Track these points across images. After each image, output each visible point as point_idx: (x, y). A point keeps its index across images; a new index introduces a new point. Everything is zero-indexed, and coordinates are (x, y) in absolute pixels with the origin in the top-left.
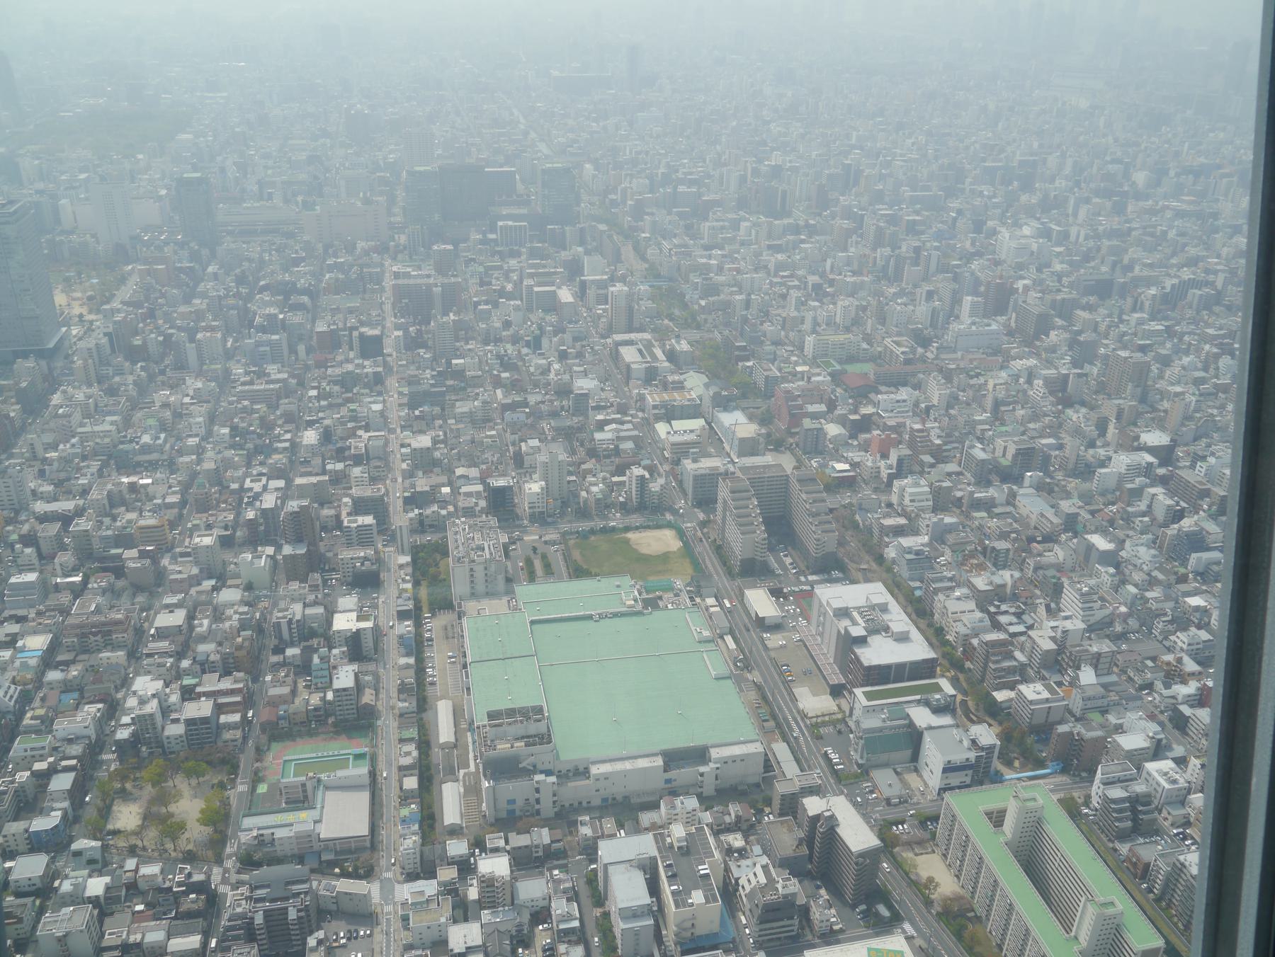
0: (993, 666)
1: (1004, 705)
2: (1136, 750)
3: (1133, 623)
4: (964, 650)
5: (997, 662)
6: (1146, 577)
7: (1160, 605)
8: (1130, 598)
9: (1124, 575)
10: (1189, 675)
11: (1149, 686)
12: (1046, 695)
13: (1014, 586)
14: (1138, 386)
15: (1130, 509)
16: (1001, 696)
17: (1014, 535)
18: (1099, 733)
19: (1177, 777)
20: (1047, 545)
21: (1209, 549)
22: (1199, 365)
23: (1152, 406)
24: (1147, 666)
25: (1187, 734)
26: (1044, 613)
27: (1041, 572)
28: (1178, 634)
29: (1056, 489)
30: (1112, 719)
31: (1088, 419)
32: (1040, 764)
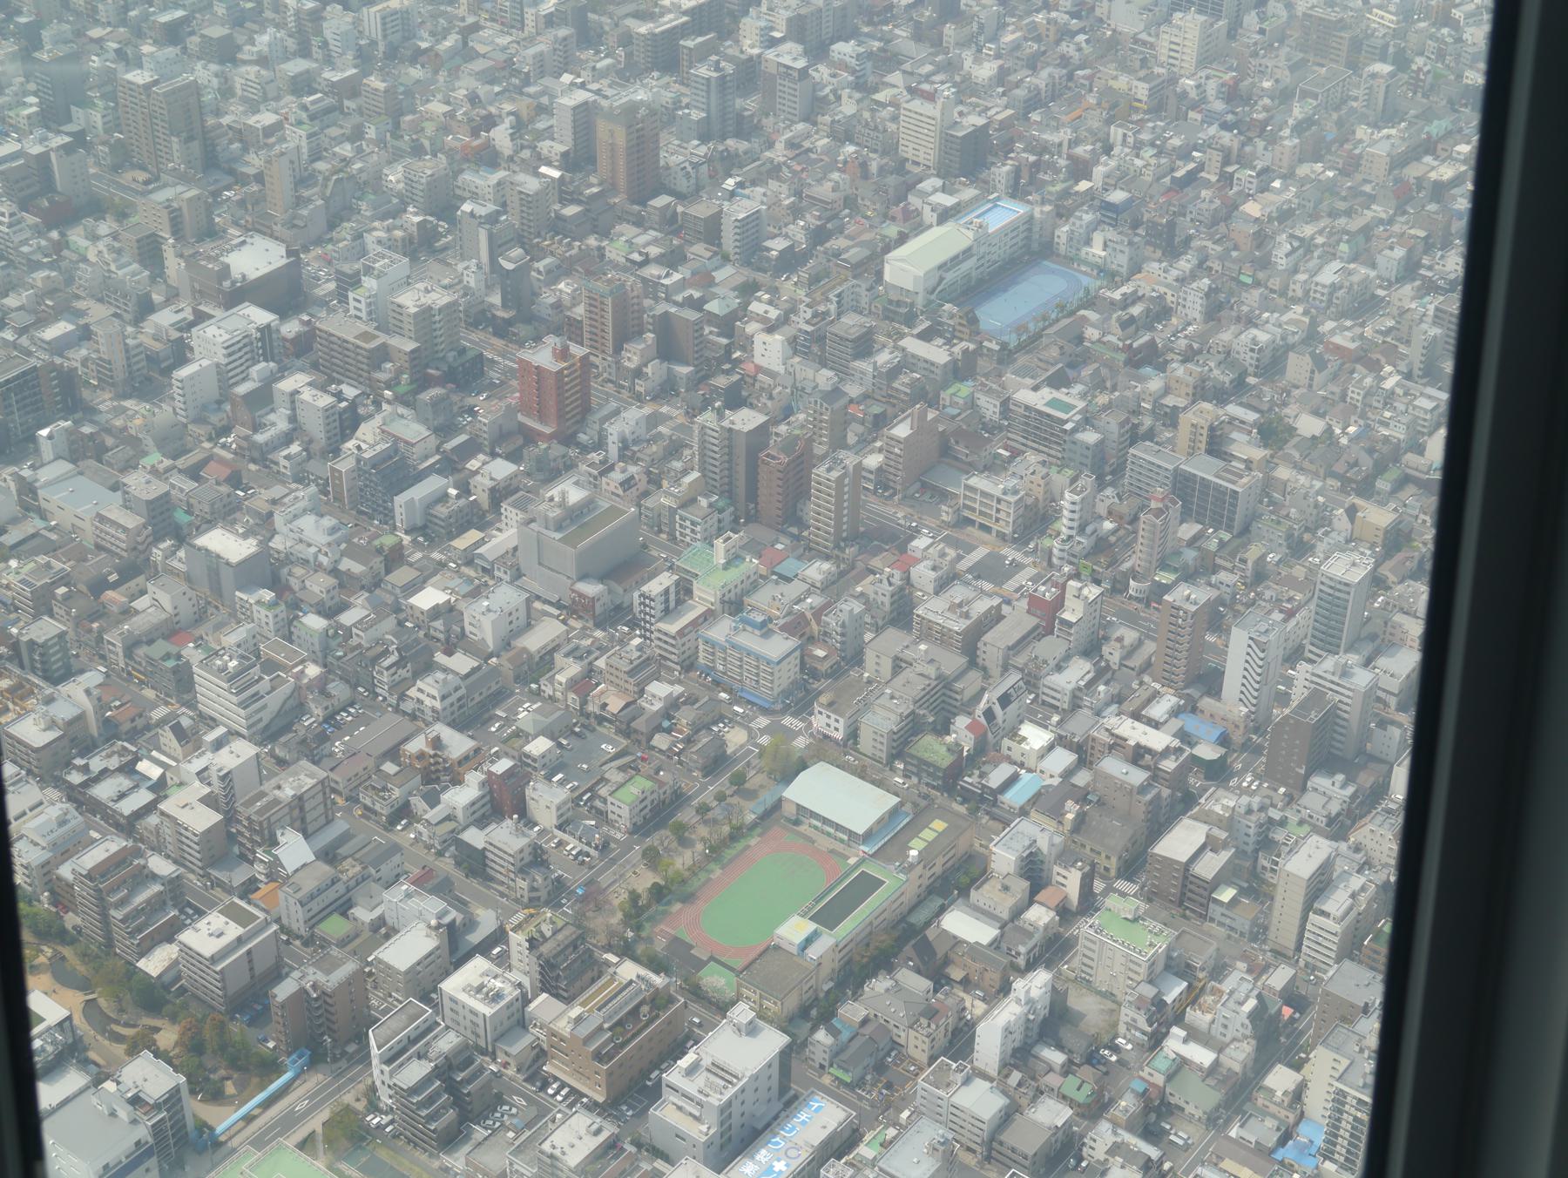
0: (117, 914)
1: (166, 979)
2: (419, 963)
3: (338, 689)
4: (52, 892)
5: (123, 902)
6: (332, 581)
7: (373, 633)
8: (316, 641)
9: (289, 588)
10: (460, 763)
11: (403, 812)
12: (234, 931)
13: (101, 706)
14: (190, 139)
15: (260, 438)
16: (154, 964)
17: (62, 590)
18: (349, 967)
19: (498, 984)
20: (132, 584)
21: (420, 476)
22: (291, 44)
23: (231, 172)
24: (387, 776)
25: (492, 879)
26: (175, 743)
27: (141, 652)
28: (419, 684)
29: (109, 441)
30: (364, 914)
31: (119, 252)
32: (270, 1068)
